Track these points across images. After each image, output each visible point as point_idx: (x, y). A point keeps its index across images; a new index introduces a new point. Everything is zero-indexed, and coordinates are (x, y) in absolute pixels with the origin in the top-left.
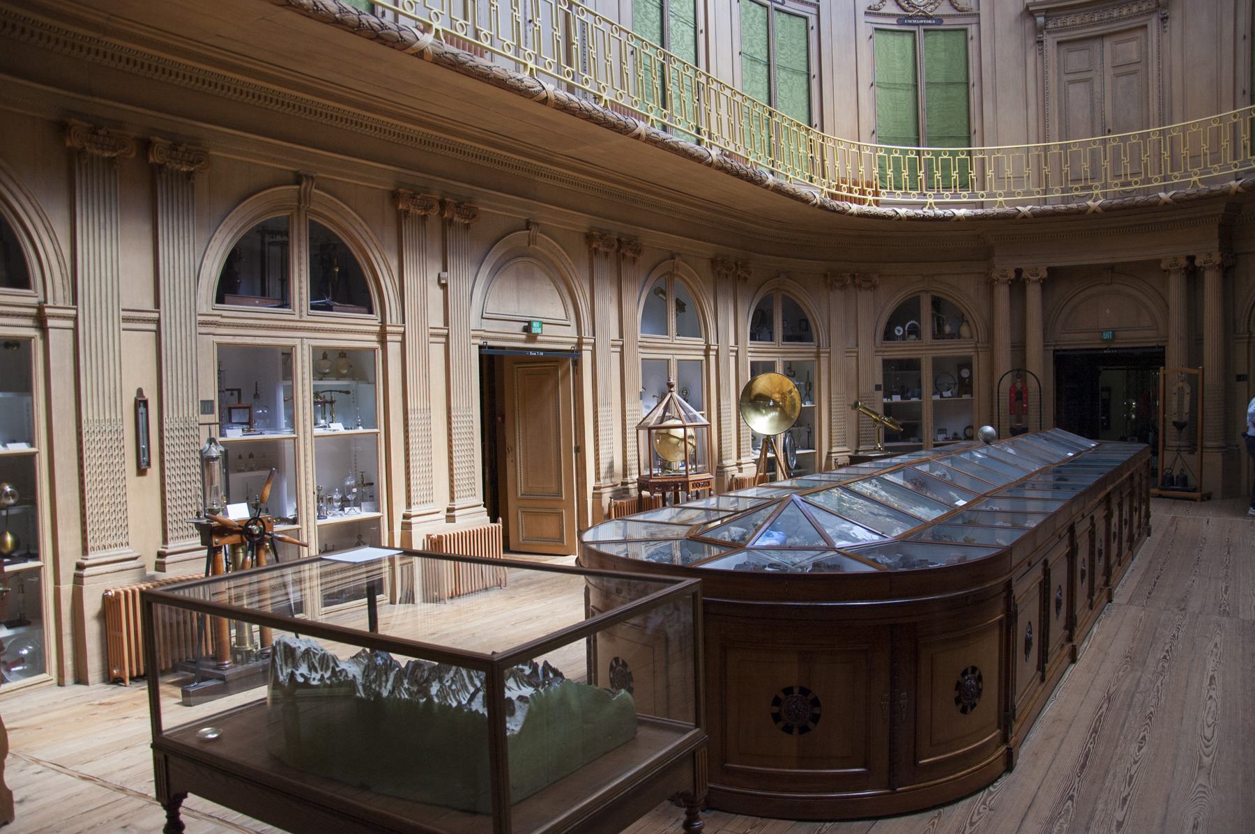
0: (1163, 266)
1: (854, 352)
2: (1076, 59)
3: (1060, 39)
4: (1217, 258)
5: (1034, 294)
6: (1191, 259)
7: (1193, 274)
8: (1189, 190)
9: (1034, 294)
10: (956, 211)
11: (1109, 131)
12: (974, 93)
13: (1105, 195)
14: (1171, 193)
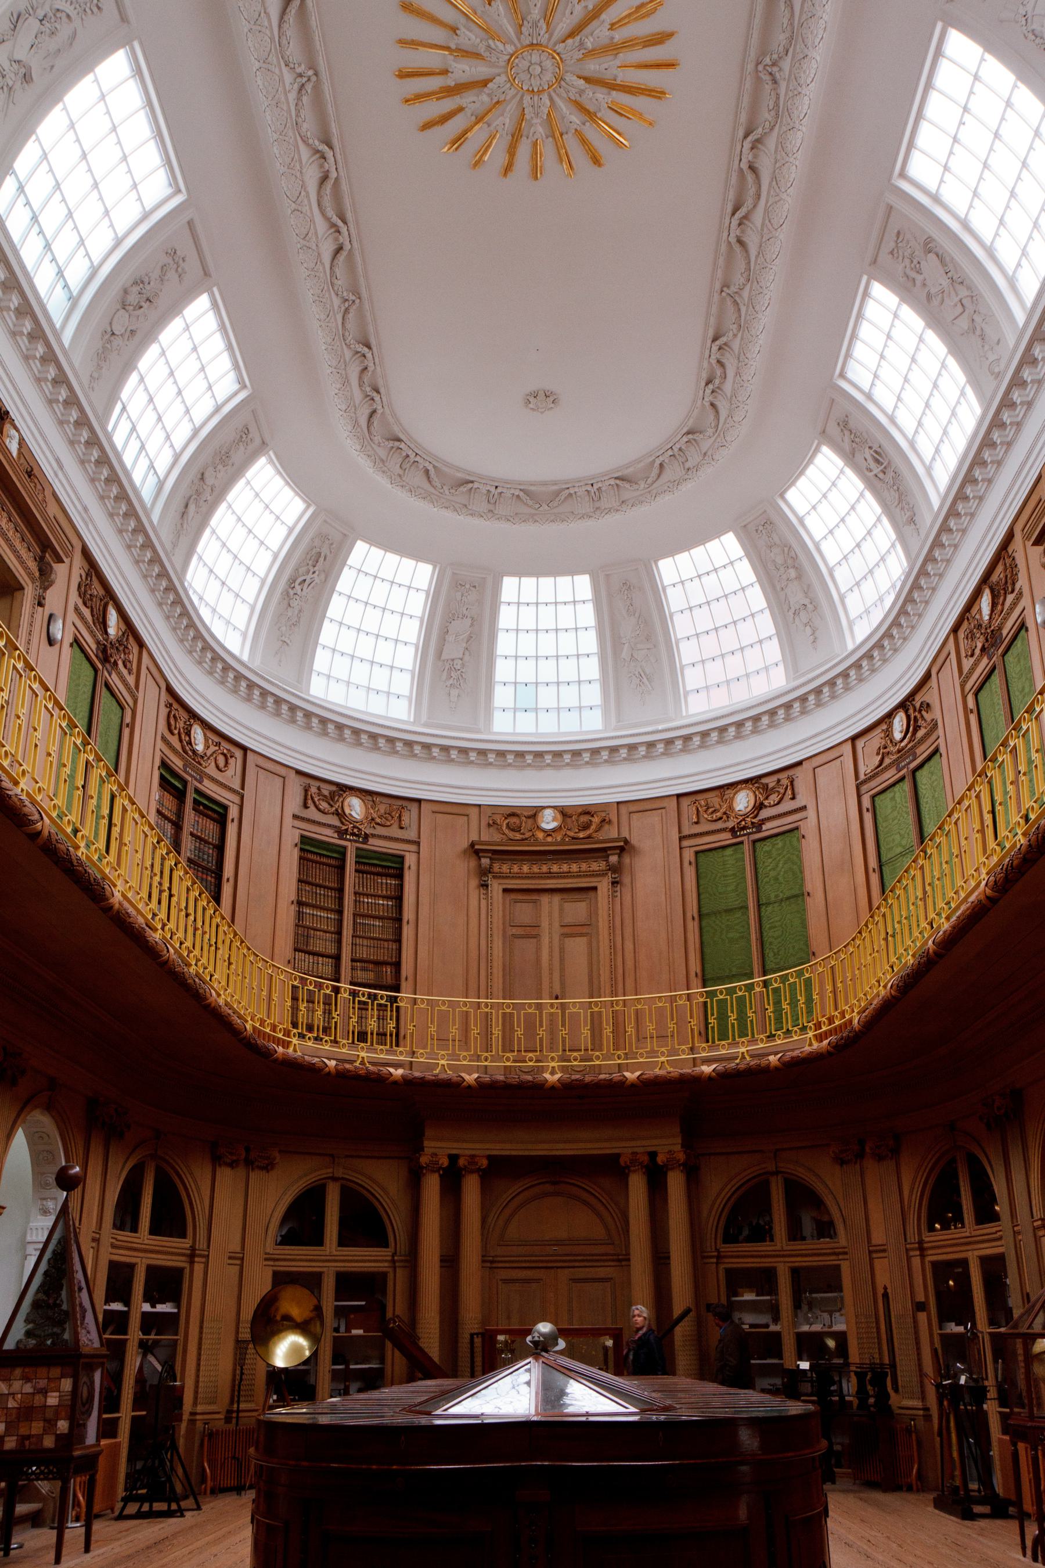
0: (622, 1163)
2: (524, 912)
3: (505, 886)
4: (681, 1157)
5: (471, 1189)
6: (653, 1155)
8: (658, 1071)
9: (471, 1189)
10: (392, 1070)
11: (557, 998)
12: (407, 932)
13: (563, 1069)
14: (638, 1073)
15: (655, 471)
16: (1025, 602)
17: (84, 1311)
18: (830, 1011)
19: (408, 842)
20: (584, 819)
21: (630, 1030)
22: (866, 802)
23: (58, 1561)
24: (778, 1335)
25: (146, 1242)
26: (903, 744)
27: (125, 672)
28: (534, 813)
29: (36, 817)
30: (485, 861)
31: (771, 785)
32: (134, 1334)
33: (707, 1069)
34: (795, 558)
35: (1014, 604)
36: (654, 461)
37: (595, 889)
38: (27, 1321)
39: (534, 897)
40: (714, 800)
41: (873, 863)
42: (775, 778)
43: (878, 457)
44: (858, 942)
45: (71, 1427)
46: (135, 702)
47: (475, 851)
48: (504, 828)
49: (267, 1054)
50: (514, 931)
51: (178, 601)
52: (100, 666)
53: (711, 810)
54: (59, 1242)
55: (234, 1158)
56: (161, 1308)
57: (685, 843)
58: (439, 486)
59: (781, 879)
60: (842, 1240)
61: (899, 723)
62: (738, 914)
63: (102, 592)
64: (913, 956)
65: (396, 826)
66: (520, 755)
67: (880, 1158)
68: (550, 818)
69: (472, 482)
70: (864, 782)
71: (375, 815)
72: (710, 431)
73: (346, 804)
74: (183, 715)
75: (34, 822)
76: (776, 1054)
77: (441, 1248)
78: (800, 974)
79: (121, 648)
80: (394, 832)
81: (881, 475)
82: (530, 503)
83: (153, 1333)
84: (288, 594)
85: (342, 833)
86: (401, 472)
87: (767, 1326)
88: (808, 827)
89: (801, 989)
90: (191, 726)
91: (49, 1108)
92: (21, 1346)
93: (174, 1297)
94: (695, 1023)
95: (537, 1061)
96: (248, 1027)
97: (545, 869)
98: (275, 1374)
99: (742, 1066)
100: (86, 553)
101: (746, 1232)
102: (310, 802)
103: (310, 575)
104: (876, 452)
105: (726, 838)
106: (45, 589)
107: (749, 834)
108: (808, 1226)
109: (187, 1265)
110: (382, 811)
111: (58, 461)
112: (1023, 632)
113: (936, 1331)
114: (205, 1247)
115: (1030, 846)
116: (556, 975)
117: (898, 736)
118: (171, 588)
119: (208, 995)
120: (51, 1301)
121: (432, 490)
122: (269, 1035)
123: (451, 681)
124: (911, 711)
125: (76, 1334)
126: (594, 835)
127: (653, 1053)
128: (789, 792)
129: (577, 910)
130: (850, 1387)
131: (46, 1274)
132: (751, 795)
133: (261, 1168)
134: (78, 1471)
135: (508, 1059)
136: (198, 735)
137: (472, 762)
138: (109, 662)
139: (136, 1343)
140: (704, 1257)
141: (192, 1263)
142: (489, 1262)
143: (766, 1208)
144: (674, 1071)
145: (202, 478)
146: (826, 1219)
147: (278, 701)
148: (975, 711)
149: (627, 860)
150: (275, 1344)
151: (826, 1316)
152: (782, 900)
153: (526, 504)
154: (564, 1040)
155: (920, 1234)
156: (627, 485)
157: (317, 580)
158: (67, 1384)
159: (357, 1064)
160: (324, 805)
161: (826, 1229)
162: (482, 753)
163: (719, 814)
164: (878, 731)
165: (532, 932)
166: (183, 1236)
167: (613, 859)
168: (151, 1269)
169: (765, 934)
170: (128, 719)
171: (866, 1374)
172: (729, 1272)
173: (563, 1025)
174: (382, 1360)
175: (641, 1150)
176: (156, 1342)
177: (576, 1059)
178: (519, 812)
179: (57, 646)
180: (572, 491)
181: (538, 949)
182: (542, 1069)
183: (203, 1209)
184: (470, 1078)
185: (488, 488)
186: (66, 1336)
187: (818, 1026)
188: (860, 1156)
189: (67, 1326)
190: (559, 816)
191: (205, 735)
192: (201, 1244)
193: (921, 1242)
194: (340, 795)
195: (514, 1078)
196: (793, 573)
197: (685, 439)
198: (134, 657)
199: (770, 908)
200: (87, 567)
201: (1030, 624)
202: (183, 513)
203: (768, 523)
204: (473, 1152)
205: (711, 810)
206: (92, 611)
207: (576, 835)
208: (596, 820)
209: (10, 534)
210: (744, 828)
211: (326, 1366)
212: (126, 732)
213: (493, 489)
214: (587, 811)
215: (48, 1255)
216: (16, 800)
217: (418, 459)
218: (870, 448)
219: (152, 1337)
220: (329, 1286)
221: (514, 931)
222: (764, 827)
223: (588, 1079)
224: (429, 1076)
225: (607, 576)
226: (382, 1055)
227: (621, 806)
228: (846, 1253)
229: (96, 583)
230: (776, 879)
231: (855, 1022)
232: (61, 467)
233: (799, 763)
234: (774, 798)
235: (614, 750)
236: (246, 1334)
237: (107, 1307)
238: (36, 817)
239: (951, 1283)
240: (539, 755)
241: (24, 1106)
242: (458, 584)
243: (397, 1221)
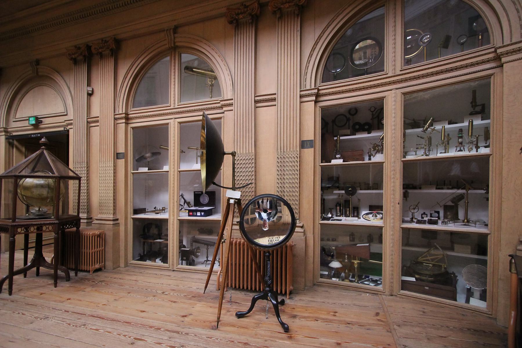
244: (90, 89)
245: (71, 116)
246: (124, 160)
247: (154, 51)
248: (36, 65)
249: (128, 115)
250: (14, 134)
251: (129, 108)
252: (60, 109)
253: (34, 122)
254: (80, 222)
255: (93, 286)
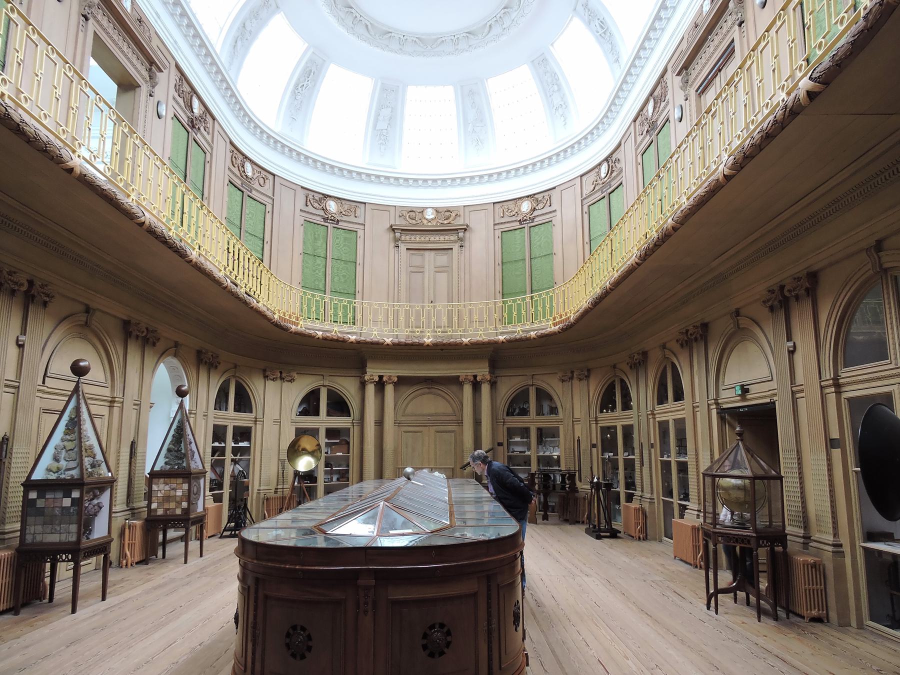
1: (278, 422)
2: (417, 259)
4: (489, 378)
6: (475, 377)
7: (476, 386)
8: (478, 339)
10: (350, 336)
11: (432, 302)
12: (359, 269)
13: (434, 337)
15: (486, 30)
16: (670, 107)
17: (193, 453)
18: (561, 311)
19: (359, 224)
20: (448, 214)
21: (466, 318)
22: (586, 209)
23: (186, 562)
24: (529, 456)
25: (232, 415)
26: (605, 179)
27: (205, 133)
28: (422, 211)
29: (141, 214)
30: (398, 235)
31: (539, 199)
32: (229, 456)
33: (501, 338)
34: (558, 80)
35: (665, 108)
36: (486, 24)
37: (452, 249)
38: (166, 457)
39: (422, 252)
40: (511, 205)
41: (587, 239)
42: (542, 195)
43: (602, 24)
44: (575, 279)
45: (189, 505)
46: (212, 149)
47: (393, 229)
48: (408, 217)
49: (286, 329)
50: (412, 269)
51: (233, 95)
52: (190, 130)
53: (510, 211)
54: (179, 422)
55: (275, 377)
56: (241, 444)
57: (496, 227)
58: (373, 34)
59: (542, 245)
60: (561, 415)
61: (604, 168)
62: (521, 263)
63: (189, 89)
64: (600, 288)
65: (353, 215)
66: (416, 180)
67: (580, 380)
68: (430, 213)
69: (391, 33)
70: (585, 198)
71: (342, 211)
72: (516, 7)
73: (327, 204)
74: (241, 157)
75: (139, 217)
76: (533, 331)
77: (375, 417)
78: (548, 293)
79: (202, 120)
80: (352, 219)
81: (603, 35)
82: (422, 45)
83: (239, 455)
84: (295, 92)
85: (325, 219)
86: (353, 26)
87: (525, 452)
88: (557, 221)
89: (547, 300)
90: (244, 162)
91: (175, 355)
92: (163, 469)
93: (248, 439)
94: (497, 316)
95: (421, 332)
96: (276, 317)
97: (427, 239)
98: (297, 473)
99: (518, 337)
100: (178, 67)
101: (517, 411)
102: (309, 203)
103: (306, 82)
104: (601, 22)
105: (517, 225)
106: (153, 87)
107: (528, 223)
108: (546, 409)
109: (254, 425)
110: (346, 209)
111: (157, 14)
112: (668, 122)
113: (600, 456)
114: (262, 417)
115: (658, 238)
116: (432, 291)
117: (603, 175)
118: (228, 88)
119: (252, 303)
120: (176, 449)
121: (369, 36)
122: (288, 320)
123: (381, 141)
124: (610, 163)
125: (189, 464)
126: (452, 222)
127: (476, 330)
128: (548, 202)
129: (442, 259)
130: (559, 479)
131: (173, 436)
132: (530, 203)
133: (288, 381)
134: (193, 524)
135: (407, 332)
136: (248, 167)
137: (391, 184)
138: (195, 128)
139: (230, 460)
140: (497, 422)
141: (256, 424)
142: (398, 424)
143: (527, 401)
144: (486, 339)
145: (244, 27)
146: (554, 406)
147: (291, 150)
148: (641, 164)
149: (467, 233)
150: (297, 461)
151: (552, 448)
152: (541, 257)
153: (420, 46)
154: (434, 322)
155: (596, 414)
156: (472, 37)
157: (310, 85)
158: (186, 486)
159: (333, 333)
160: (316, 205)
161: (554, 411)
162: (397, 179)
163: (514, 213)
164: (594, 172)
165: (420, 270)
166: (251, 412)
167: (461, 234)
168: (235, 428)
169: (533, 273)
170: (208, 159)
171: (566, 475)
172: (508, 429)
173: (434, 316)
174: (348, 466)
175: (470, 374)
176: (240, 460)
177: (439, 332)
178: (414, 210)
179: (163, 119)
180: (443, 39)
181: (423, 279)
182: (424, 337)
183: (260, 400)
184: (388, 341)
185: (400, 36)
186: (184, 465)
187: (554, 319)
188: (572, 378)
189: (185, 459)
190: (435, 212)
191: (252, 167)
192: (260, 416)
193: (596, 418)
194: (324, 200)
195: (409, 341)
196: (556, 87)
197: (503, 11)
198: (210, 125)
199: (536, 260)
200: (179, 75)
201: (671, 119)
202: (235, 46)
203: (545, 60)
204: (390, 374)
205: (510, 211)
206: (184, 100)
207: (443, 222)
208: (453, 215)
209: (130, 55)
210: (525, 220)
211: (322, 468)
212: (208, 165)
213: (402, 37)
214: (448, 211)
215: (174, 427)
216: (127, 205)
217: (361, 18)
218: (598, 19)
219: (238, 457)
220: (322, 434)
221: (412, 269)
222: (535, 220)
223: (445, 341)
224: (368, 340)
225: (462, 86)
226: (345, 328)
227: (467, 209)
228: (562, 422)
229: (185, 84)
230: (540, 246)
231: (572, 318)
232: (159, 17)
233: (555, 188)
234: (541, 206)
235: (463, 179)
236: (284, 456)
237: (213, 445)
238: (141, 214)
239: (608, 436)
240: (425, 181)
241: (162, 354)
242: (384, 89)
243: (354, 404)
244: (791, 344)
245: (774, 385)
246: (839, 450)
247: (856, 282)
248: (736, 317)
249: (838, 379)
250: (725, 406)
251: (839, 369)
252: (764, 373)
253: (740, 392)
254: (786, 539)
255: (799, 634)
